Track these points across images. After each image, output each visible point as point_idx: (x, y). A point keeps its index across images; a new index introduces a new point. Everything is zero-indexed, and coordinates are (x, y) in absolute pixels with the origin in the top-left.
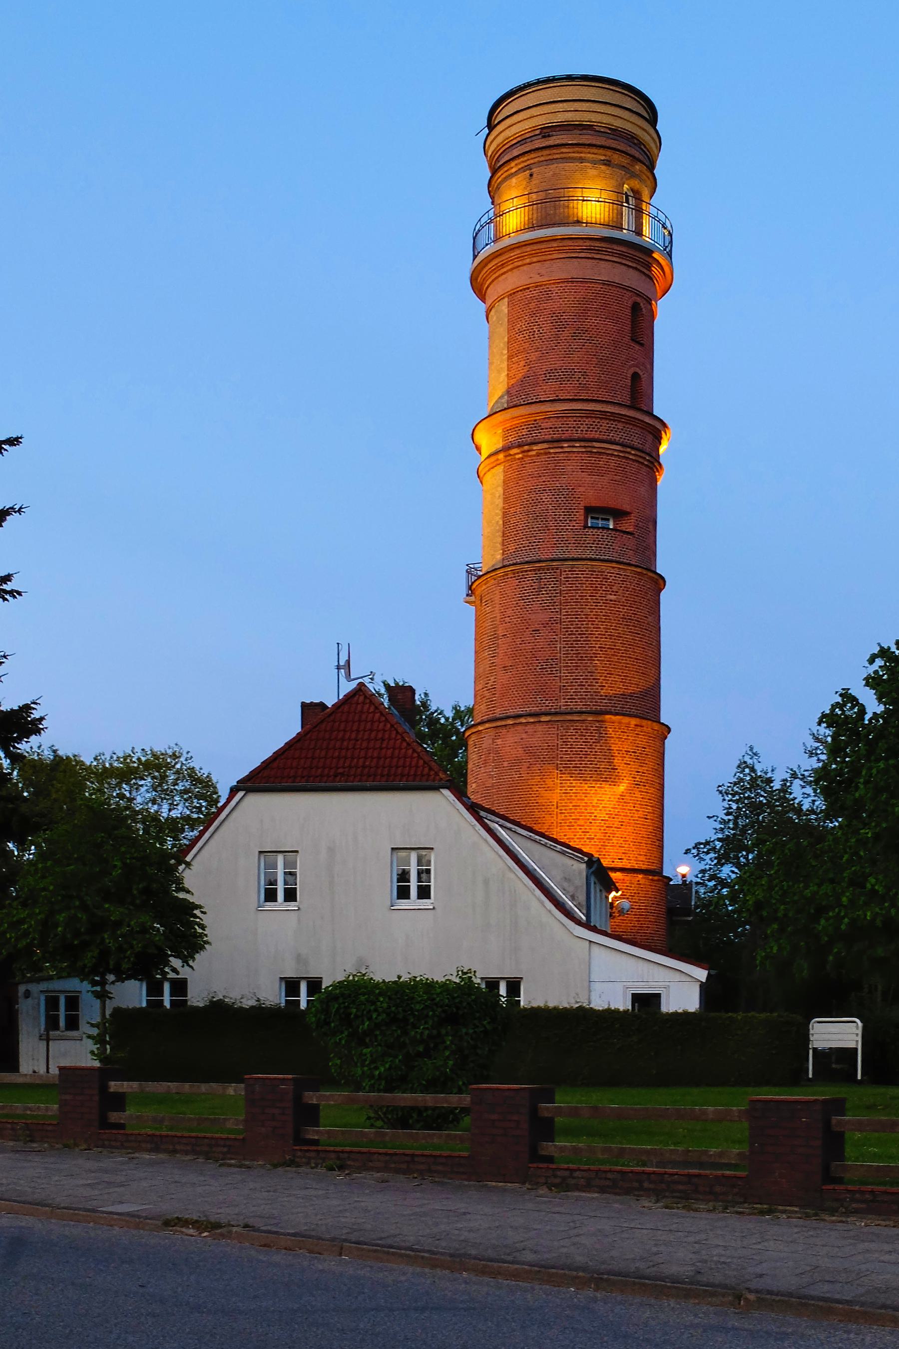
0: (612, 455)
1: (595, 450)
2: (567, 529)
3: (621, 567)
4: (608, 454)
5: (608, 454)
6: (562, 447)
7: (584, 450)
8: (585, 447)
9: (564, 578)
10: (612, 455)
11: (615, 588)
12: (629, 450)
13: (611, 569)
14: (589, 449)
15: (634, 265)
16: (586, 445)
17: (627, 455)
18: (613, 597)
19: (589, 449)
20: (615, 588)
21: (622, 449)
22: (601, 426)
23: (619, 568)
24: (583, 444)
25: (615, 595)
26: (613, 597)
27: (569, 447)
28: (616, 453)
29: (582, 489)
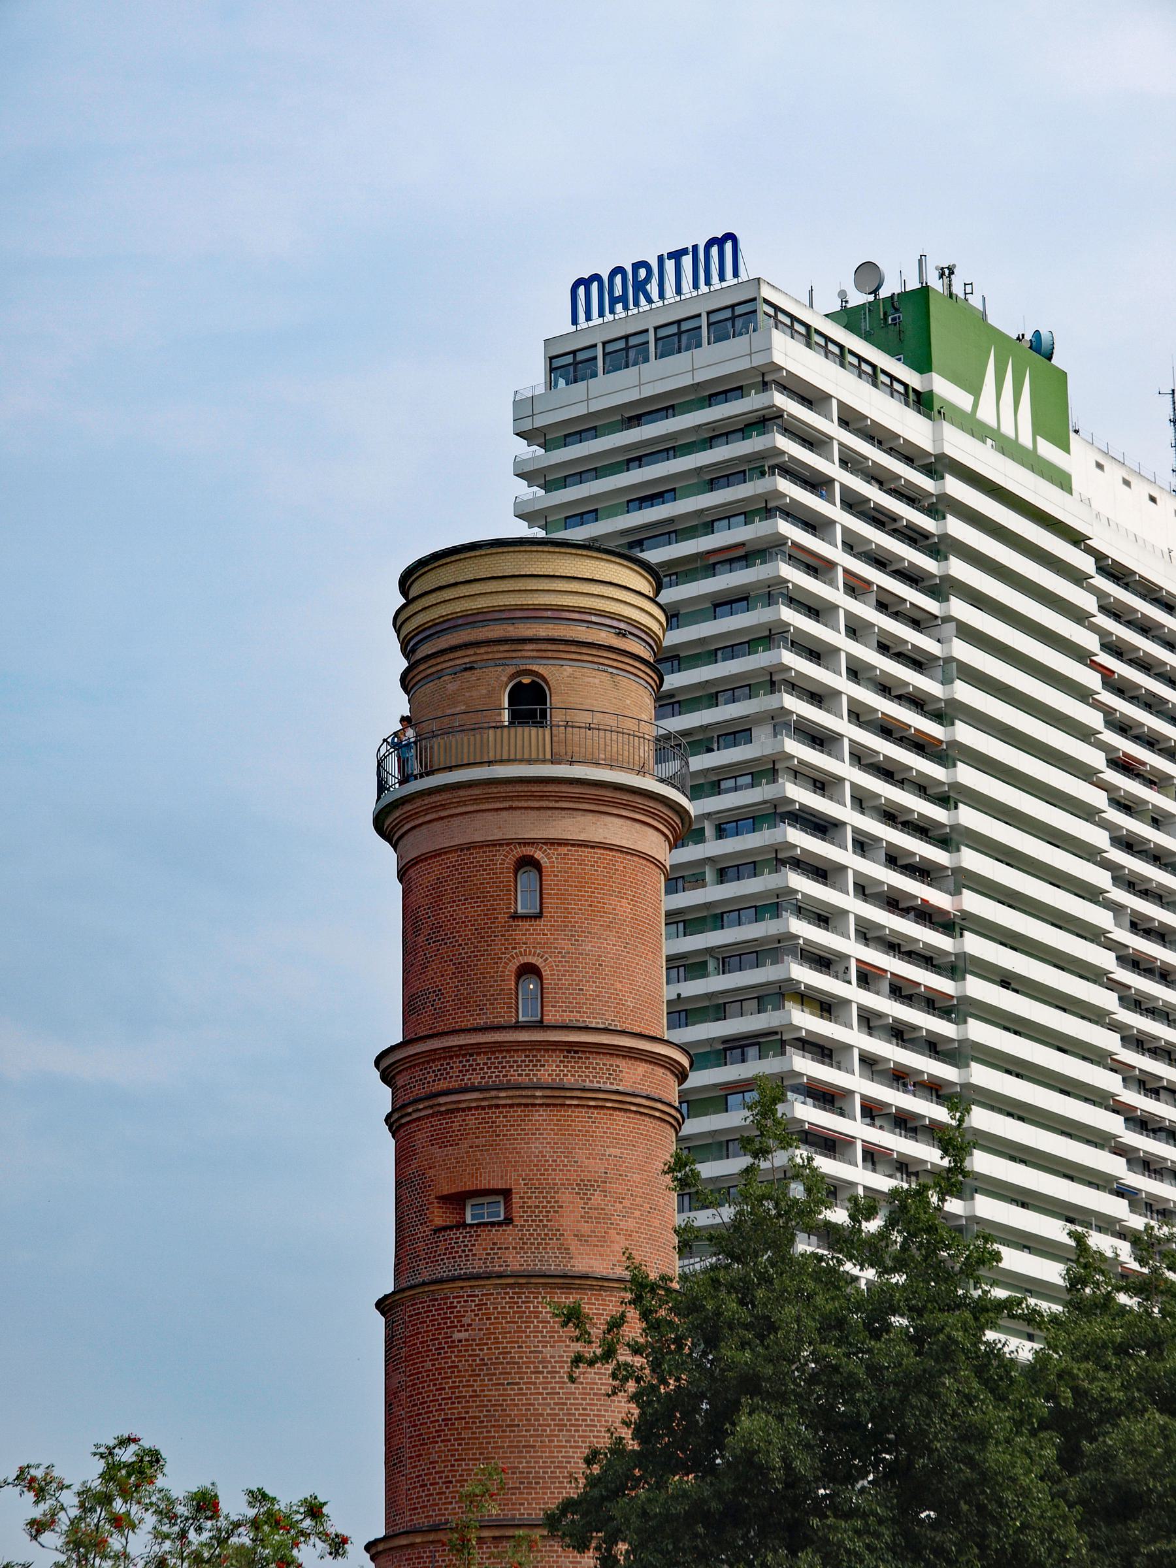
0: (470, 1109)
1: (443, 1109)
2: (418, 1238)
3: (471, 1284)
4: (463, 1110)
5: (463, 1110)
6: (410, 1114)
7: (431, 1112)
8: (431, 1107)
9: (409, 1317)
10: (470, 1109)
11: (466, 1321)
12: (493, 1093)
13: (458, 1290)
14: (436, 1109)
15: (506, 805)
16: (431, 1103)
17: (493, 1102)
18: (463, 1335)
19: (436, 1109)
20: (466, 1321)
21: (481, 1096)
22: (452, 1068)
23: (471, 1287)
24: (427, 1104)
25: (467, 1330)
26: (463, 1335)
27: (414, 1111)
28: (474, 1105)
29: (432, 1172)
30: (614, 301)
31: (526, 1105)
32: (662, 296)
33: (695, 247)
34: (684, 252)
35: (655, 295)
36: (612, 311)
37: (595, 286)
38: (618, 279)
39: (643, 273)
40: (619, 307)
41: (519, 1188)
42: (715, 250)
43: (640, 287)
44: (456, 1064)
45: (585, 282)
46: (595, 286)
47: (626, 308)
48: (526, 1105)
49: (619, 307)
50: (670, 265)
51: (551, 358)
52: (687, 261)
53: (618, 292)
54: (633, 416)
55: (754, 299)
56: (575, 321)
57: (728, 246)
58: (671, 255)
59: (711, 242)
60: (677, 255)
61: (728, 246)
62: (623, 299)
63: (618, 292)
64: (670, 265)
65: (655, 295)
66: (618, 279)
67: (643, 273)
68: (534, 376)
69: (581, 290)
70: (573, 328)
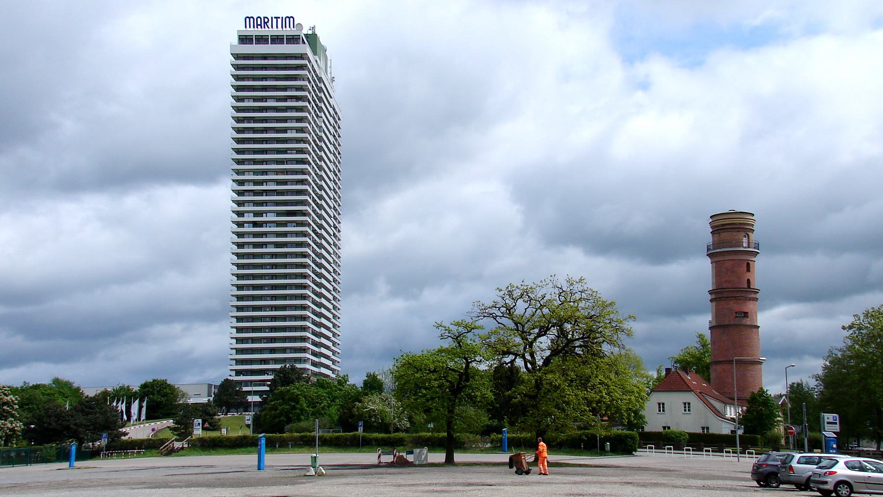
30: (257, 25)
32: (272, 27)
33: (282, 18)
34: (279, 18)
35: (270, 26)
36: (257, 27)
37: (252, 20)
38: (259, 19)
39: (266, 20)
40: (259, 27)
41: (749, 312)
42: (288, 19)
44: (739, 293)
45: (249, 18)
46: (252, 20)
47: (261, 27)
50: (275, 20)
51: (239, 36)
52: (280, 21)
53: (259, 23)
54: (265, 57)
55: (299, 35)
56: (246, 27)
57: (292, 19)
58: (275, 18)
60: (277, 18)
61: (292, 19)
62: (261, 25)
63: (259, 23)
64: (275, 20)
65: (270, 26)
66: (259, 19)
67: (266, 20)
68: (235, 41)
69: (248, 20)
70: (245, 29)
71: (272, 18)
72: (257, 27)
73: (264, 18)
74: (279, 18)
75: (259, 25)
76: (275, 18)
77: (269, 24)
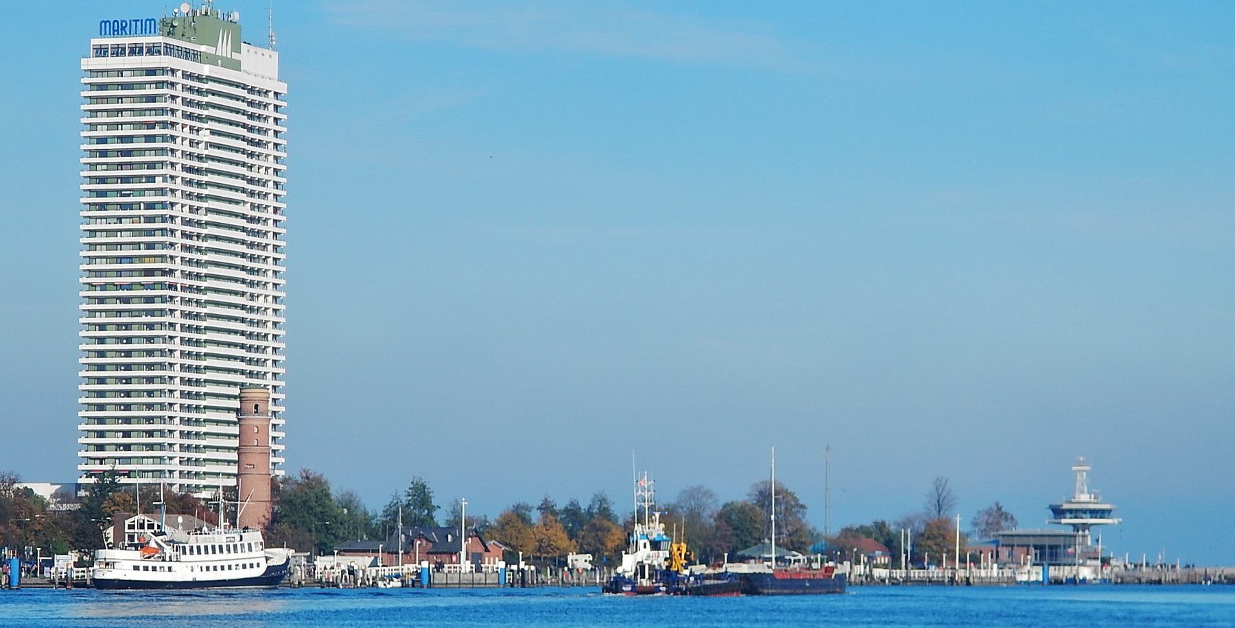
30: (114, 31)
31: (37, 584)
33: (142, 20)
34: (139, 20)
35: (128, 33)
37: (108, 24)
38: (116, 23)
40: (116, 33)
42: (148, 23)
43: (123, 28)
45: (105, 22)
46: (108, 24)
48: (37, 584)
49: (116, 33)
50: (133, 23)
52: (139, 23)
53: (116, 28)
57: (153, 22)
58: (134, 21)
59: (147, 20)
60: (136, 21)
61: (153, 22)
62: (118, 31)
63: (116, 28)
64: (133, 23)
65: (128, 33)
66: (116, 23)
69: (103, 24)
71: (130, 21)
72: (114, 34)
73: (122, 21)
74: (139, 20)
75: (116, 31)
76: (134, 21)
77: (127, 29)
